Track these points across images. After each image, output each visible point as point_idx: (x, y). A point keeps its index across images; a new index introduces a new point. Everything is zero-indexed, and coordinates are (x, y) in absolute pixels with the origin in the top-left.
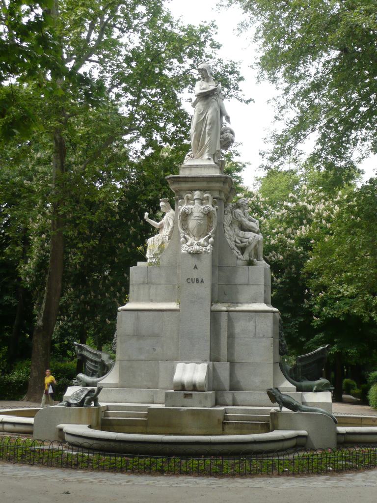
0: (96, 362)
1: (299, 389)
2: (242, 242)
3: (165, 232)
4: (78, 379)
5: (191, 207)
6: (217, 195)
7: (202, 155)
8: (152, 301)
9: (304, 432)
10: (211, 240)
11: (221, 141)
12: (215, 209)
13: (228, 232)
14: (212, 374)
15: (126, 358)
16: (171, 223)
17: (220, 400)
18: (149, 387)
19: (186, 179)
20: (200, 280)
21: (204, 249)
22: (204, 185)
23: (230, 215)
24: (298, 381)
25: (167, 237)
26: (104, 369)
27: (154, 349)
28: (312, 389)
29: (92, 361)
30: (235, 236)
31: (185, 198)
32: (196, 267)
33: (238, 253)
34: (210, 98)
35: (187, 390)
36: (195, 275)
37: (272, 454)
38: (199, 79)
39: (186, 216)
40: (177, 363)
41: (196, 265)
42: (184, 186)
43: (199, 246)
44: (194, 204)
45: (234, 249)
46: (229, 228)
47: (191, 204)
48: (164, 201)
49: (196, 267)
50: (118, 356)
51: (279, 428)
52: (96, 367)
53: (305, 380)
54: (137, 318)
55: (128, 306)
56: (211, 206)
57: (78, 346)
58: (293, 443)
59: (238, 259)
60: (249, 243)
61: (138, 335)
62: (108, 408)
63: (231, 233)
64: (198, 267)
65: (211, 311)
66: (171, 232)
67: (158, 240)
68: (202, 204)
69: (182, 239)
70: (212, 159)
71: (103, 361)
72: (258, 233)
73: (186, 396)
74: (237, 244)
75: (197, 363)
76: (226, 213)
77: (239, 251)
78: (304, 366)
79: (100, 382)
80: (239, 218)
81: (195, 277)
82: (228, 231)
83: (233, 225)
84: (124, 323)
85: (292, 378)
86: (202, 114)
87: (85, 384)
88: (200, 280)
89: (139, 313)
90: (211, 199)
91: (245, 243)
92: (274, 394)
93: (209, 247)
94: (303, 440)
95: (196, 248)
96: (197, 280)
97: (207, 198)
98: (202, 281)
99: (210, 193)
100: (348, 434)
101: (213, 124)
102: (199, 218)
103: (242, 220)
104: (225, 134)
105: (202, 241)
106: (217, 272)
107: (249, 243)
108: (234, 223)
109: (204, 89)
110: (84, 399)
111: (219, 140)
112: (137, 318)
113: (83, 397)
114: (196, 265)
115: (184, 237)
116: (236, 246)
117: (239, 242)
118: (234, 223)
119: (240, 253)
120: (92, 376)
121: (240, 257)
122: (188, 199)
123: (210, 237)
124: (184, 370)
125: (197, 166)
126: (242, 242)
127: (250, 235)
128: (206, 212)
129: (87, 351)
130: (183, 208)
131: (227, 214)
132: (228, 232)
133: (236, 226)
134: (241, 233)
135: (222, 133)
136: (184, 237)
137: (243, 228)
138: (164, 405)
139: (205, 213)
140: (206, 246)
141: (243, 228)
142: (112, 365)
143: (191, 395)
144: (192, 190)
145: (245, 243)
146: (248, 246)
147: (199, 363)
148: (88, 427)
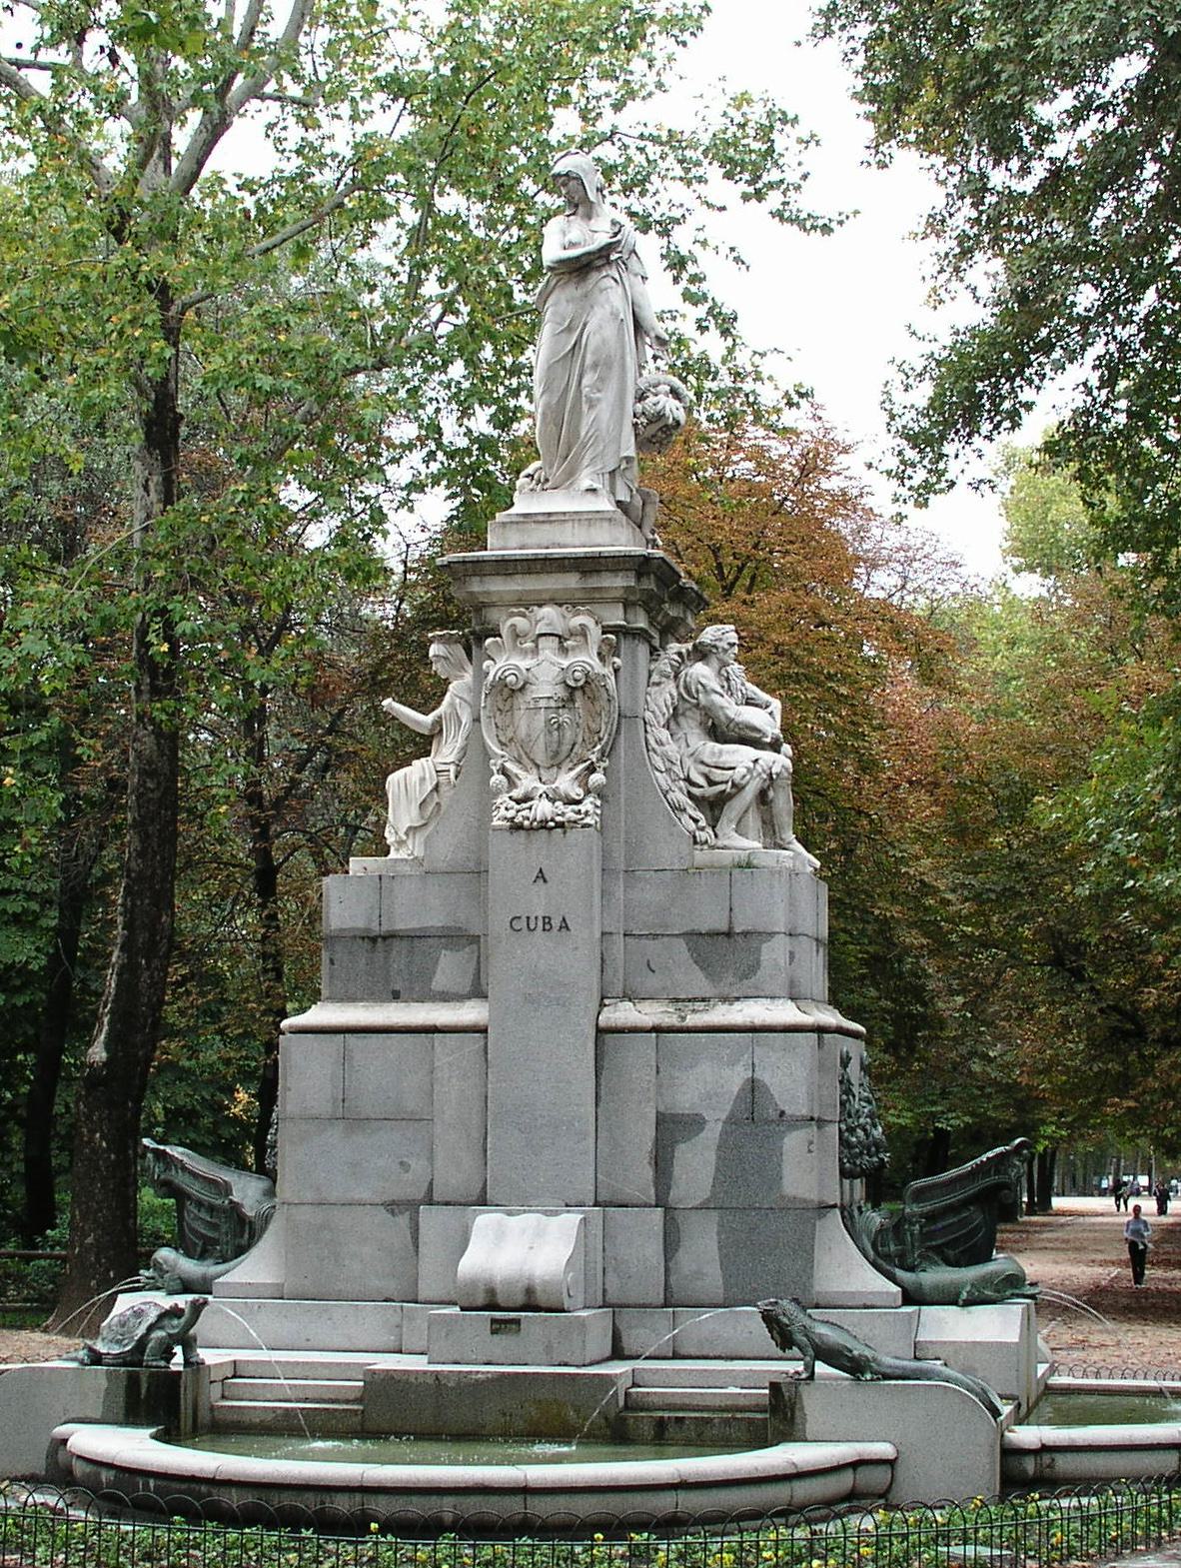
0: (212, 1209)
1: (911, 1297)
2: (711, 783)
3: (446, 752)
4: (158, 1267)
6: (616, 617)
7: (571, 474)
8: (396, 996)
9: (883, 1449)
10: (597, 778)
11: (635, 425)
12: (608, 671)
14: (597, 1254)
15: (309, 1196)
16: (466, 718)
17: (629, 1343)
18: (387, 1295)
19: (506, 567)
20: (556, 923)
21: (570, 813)
22: (572, 581)
23: (670, 686)
24: (911, 1269)
25: (452, 768)
26: (237, 1234)
27: (401, 1163)
28: (958, 1294)
29: (200, 1204)
30: (688, 762)
31: (504, 631)
32: (541, 876)
33: (696, 821)
34: (594, 276)
35: (508, 1308)
36: (538, 903)
37: (719, 1527)
38: (558, 212)
39: (509, 692)
40: (476, 1214)
42: (498, 586)
43: (553, 801)
44: (535, 651)
46: (664, 734)
47: (524, 653)
48: (445, 640)
49: (541, 876)
50: (285, 1188)
51: (810, 1429)
52: (214, 1227)
53: (936, 1264)
54: (345, 1058)
55: (319, 1015)
56: (596, 662)
57: (155, 1151)
58: (845, 1482)
60: (734, 785)
61: (348, 1117)
62: (237, 1370)
63: (672, 749)
65: (601, 1031)
66: (464, 750)
67: (423, 779)
68: (564, 651)
70: (604, 492)
71: (235, 1207)
72: (775, 747)
73: (498, 1327)
74: (696, 791)
75: (545, 1213)
76: (655, 678)
77: (698, 815)
78: (931, 1217)
79: (221, 1280)
81: (540, 914)
82: (660, 743)
83: (681, 719)
84: (306, 1077)
85: (887, 1257)
86: (569, 329)
87: (177, 1285)
88: (556, 923)
89: (351, 1038)
90: (595, 633)
91: (722, 787)
92: (785, 1320)
94: (878, 1478)
95: (543, 809)
96: (547, 920)
97: (583, 631)
98: (564, 926)
99: (590, 613)
100: (1045, 1449)
101: (608, 365)
102: (553, 704)
103: (713, 703)
104: (652, 399)
105: (566, 782)
106: (620, 893)
107: (734, 785)
108: (683, 714)
109: (572, 245)
110: (142, 1343)
111: (629, 420)
112: (345, 1058)
113: (141, 1331)
115: (504, 771)
116: (690, 795)
117: (701, 781)
118: (683, 714)
119: (702, 823)
120: (202, 1256)
121: (702, 836)
122: (516, 635)
123: (591, 769)
124: (500, 1235)
125: (548, 518)
126: (711, 783)
127: (740, 756)
128: (576, 680)
129: (184, 1169)
130: (503, 663)
131: (658, 684)
133: (693, 724)
134: (711, 749)
135: (641, 397)
136: (504, 771)
137: (720, 731)
138: (424, 1359)
139: (571, 683)
140: (578, 802)
141: (720, 731)
142: (266, 1219)
143: (517, 1322)
144: (527, 603)
145: (722, 787)
146: (731, 797)
147: (556, 1213)
148: (154, 1437)
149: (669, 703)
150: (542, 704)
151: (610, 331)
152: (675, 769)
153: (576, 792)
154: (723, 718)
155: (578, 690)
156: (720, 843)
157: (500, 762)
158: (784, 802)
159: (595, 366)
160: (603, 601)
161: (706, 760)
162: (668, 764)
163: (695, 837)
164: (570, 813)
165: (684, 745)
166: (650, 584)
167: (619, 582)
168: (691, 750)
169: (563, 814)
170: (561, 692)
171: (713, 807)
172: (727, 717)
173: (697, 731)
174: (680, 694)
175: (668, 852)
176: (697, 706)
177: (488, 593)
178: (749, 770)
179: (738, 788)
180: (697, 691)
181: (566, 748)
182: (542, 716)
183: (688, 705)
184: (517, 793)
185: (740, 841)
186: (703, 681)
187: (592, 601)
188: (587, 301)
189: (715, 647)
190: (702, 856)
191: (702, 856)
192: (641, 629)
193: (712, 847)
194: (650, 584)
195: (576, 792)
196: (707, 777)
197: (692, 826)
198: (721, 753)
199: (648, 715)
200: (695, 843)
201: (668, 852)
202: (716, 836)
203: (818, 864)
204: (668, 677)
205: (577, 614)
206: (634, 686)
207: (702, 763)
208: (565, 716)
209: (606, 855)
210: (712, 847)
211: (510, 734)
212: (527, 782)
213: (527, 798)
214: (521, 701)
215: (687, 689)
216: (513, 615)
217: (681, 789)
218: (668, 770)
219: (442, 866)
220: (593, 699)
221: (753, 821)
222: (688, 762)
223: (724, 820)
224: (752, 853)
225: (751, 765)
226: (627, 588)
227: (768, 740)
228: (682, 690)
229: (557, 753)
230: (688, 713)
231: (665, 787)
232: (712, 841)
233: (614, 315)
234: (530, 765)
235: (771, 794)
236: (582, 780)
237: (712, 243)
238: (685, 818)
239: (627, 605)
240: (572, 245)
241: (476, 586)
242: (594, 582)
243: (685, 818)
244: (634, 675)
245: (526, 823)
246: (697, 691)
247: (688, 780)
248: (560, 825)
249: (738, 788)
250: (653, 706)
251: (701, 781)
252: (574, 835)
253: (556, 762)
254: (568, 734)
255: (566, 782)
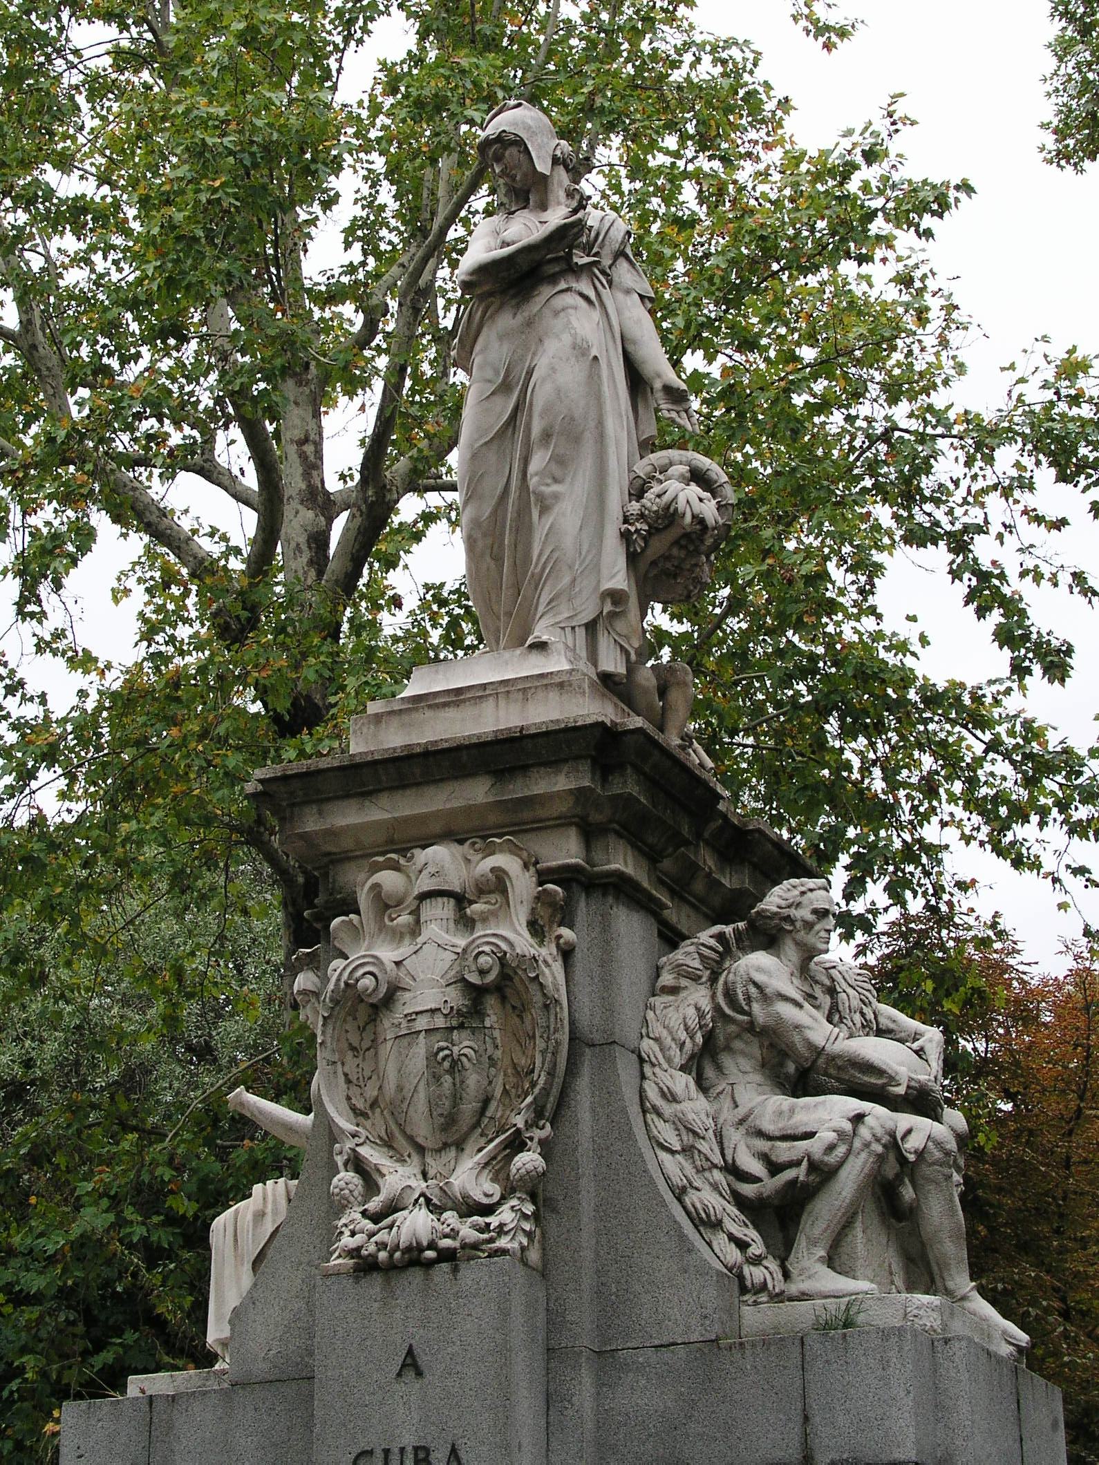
2: (775, 1168)
5: (388, 954)
6: (566, 850)
10: (528, 1160)
11: (625, 536)
12: (547, 952)
13: (667, 1109)
21: (467, 1231)
22: (477, 792)
32: (411, 1364)
33: (742, 1245)
41: (410, 1352)
42: (350, 817)
43: (436, 1209)
44: (415, 929)
45: (717, 1225)
46: (682, 1082)
47: (397, 936)
49: (411, 1364)
59: (744, 1290)
64: (423, 1360)
69: (346, 1178)
72: (920, 1102)
74: (748, 1190)
76: (667, 979)
77: (751, 1234)
80: (756, 1008)
83: (727, 1060)
86: (505, 387)
90: (523, 884)
91: (789, 1174)
93: (505, 1215)
95: (416, 1224)
97: (498, 884)
99: (515, 850)
101: (576, 439)
102: (440, 1022)
103: (779, 1018)
105: (468, 1176)
107: (814, 1166)
108: (728, 1048)
109: (505, 244)
111: (613, 526)
114: (410, 1352)
116: (740, 1201)
117: (755, 1167)
119: (757, 1248)
121: (755, 1274)
122: (385, 904)
123: (516, 1144)
125: (457, 697)
126: (775, 1168)
128: (482, 972)
131: (674, 990)
132: (667, 1109)
134: (773, 1109)
135: (638, 492)
136: (357, 1164)
137: (804, 1074)
139: (474, 978)
140: (489, 1210)
144: (401, 842)
145: (789, 1174)
149: (693, 1022)
150: (422, 1023)
151: (571, 376)
152: (703, 1146)
153: (484, 1188)
154: (800, 1047)
155: (494, 991)
156: (793, 1288)
157: (349, 1144)
158: (942, 1213)
159: (547, 436)
160: (540, 826)
161: (769, 1127)
162: (688, 1139)
163: (741, 1277)
164: (467, 1231)
165: (727, 1103)
166: (629, 786)
167: (558, 783)
168: (741, 1111)
169: (453, 1234)
170: (455, 997)
171: (780, 1215)
172: (810, 1045)
173: (758, 1078)
174: (717, 1008)
175: (678, 1308)
176: (751, 1027)
177: (332, 833)
178: (841, 1134)
179: (823, 1173)
180: (749, 999)
181: (469, 1107)
182: (420, 1048)
183: (732, 1028)
184: (374, 1204)
185: (843, 1282)
186: (759, 977)
187: (520, 828)
188: (531, 331)
189: (788, 919)
190: (756, 1317)
191: (756, 1317)
192: (619, 874)
193: (778, 1297)
194: (629, 786)
195: (484, 1188)
196: (765, 1158)
197: (733, 1255)
198: (792, 1111)
199: (647, 1046)
200: (744, 1290)
201: (678, 1308)
202: (786, 1275)
203: (1023, 1338)
204: (696, 979)
205: (489, 851)
206: (607, 982)
207: (760, 1134)
208: (464, 1044)
209: (555, 1320)
210: (778, 1297)
211: (371, 1092)
212: (398, 1177)
213: (393, 1207)
214: (390, 1024)
215: (729, 995)
216: (377, 868)
217: (715, 1187)
218: (687, 1150)
219: (260, 1368)
220: (521, 1011)
221: (868, 1241)
222: (735, 1137)
223: (801, 1242)
224: (854, 1301)
225: (848, 1126)
226: (580, 794)
227: (901, 1090)
228: (721, 1000)
229: (450, 1121)
230: (738, 1045)
231: (678, 1180)
232: (777, 1283)
233: (580, 349)
234: (407, 1148)
235: (908, 1193)
236: (498, 1166)
237: (1046, 570)
238: (720, 1241)
239: (590, 835)
240: (505, 244)
241: (311, 823)
242: (517, 789)
243: (720, 1241)
244: (607, 962)
245: (383, 1255)
246: (749, 999)
247: (733, 1170)
248: (447, 1256)
249: (823, 1173)
250: (657, 1029)
251: (755, 1167)
252: (472, 1273)
253: (453, 1137)
254: (473, 1080)
255: (468, 1176)
